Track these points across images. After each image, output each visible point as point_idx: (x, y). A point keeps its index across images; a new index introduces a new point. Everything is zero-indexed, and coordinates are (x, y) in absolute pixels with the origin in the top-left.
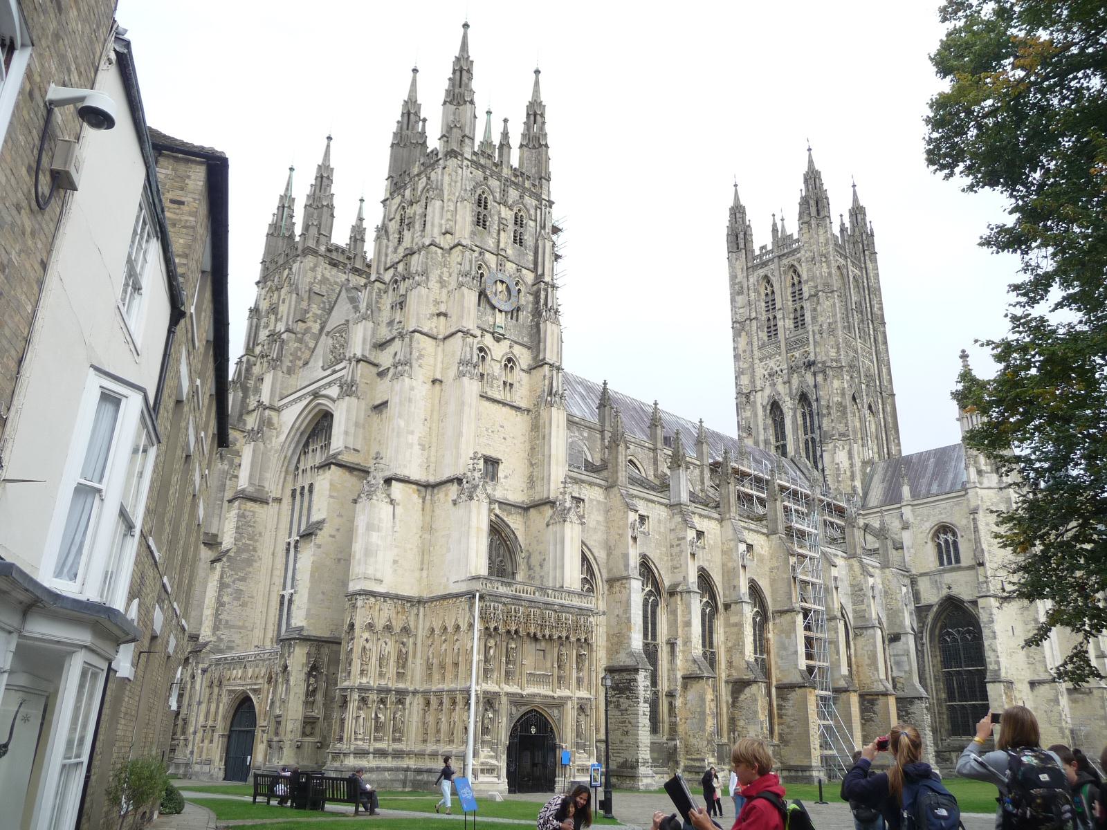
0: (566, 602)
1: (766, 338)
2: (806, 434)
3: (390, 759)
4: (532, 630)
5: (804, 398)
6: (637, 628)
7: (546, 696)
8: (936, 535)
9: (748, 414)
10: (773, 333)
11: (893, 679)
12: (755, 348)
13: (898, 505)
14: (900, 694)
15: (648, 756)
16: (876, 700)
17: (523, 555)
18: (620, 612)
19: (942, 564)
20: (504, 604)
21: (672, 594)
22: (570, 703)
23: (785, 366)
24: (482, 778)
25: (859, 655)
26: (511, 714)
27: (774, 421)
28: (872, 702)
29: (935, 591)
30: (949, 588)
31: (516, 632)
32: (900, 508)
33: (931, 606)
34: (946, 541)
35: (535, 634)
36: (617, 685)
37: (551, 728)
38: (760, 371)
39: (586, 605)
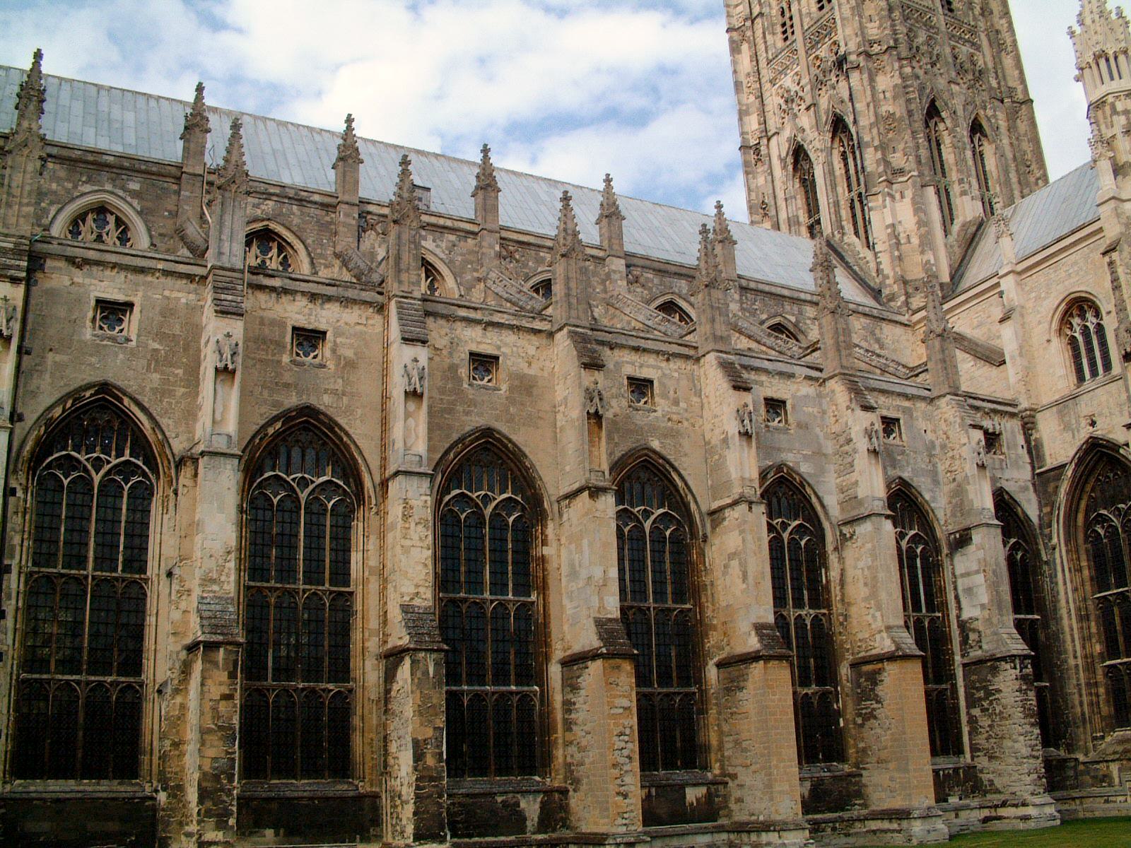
1: (780, 44)
2: (850, 191)
5: (838, 126)
8: (1065, 320)
9: (761, 180)
10: (789, 31)
11: (962, 625)
12: (763, 63)
13: (995, 280)
14: (975, 654)
16: (880, 671)
19: (1081, 378)
21: (180, 463)
23: (804, 81)
25: (849, 579)
27: (803, 182)
28: (874, 679)
29: (1068, 436)
30: (1093, 424)
32: (998, 285)
33: (1063, 466)
34: (1085, 331)
38: (773, 101)
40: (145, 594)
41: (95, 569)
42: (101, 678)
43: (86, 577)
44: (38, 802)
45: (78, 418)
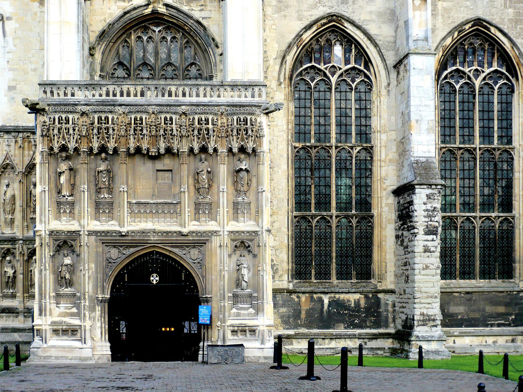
0: (206, 100)
3: (21, 318)
4: (132, 145)
6: (424, 126)
7: (167, 233)
15: (435, 310)
17: (219, 51)
18: (403, 107)
20: (83, 114)
22: (216, 241)
24: (54, 341)
26: (109, 261)
31: (103, 149)
35: (138, 150)
36: (402, 211)
37: (190, 276)
39: (249, 100)
40: (512, 159)
41: (480, 144)
42: (488, 214)
43: (475, 149)
44: (456, 294)
45: (461, 44)
